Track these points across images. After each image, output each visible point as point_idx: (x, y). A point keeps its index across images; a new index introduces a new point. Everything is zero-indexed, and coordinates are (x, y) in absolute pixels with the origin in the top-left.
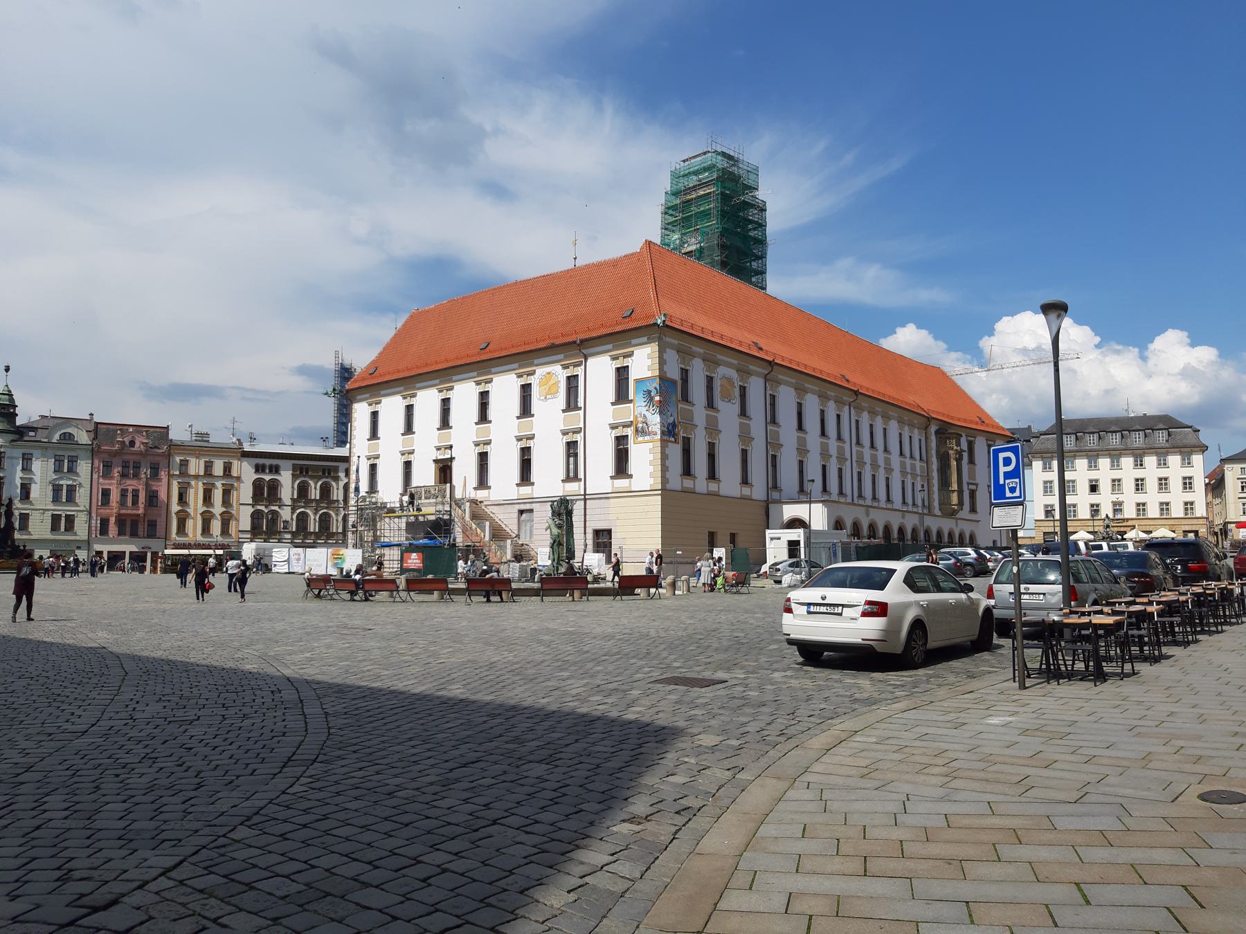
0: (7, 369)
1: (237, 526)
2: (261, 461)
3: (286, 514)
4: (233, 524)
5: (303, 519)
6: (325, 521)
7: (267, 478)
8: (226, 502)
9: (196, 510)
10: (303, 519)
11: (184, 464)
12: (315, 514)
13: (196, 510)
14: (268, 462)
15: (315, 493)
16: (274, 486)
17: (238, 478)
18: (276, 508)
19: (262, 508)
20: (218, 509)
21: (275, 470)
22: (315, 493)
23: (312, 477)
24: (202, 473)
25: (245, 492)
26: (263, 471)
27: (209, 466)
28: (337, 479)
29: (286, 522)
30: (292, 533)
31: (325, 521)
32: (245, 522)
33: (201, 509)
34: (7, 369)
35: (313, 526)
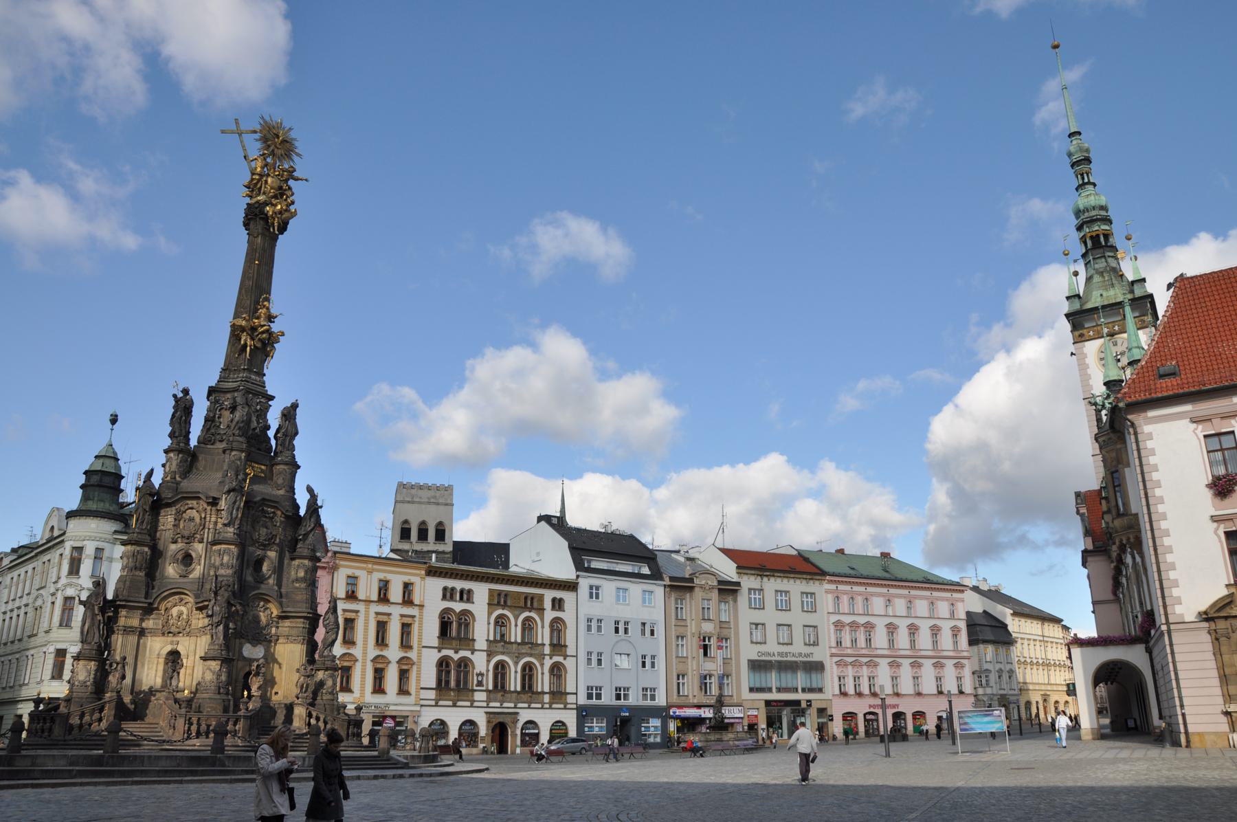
0: (114, 420)
1: (418, 680)
2: (450, 583)
3: (480, 663)
4: (413, 675)
5: (500, 669)
6: (528, 673)
7: (458, 607)
8: (405, 645)
9: (365, 653)
10: (500, 669)
11: (352, 581)
12: (516, 663)
13: (365, 653)
14: (459, 584)
15: (515, 633)
16: (465, 619)
17: (421, 606)
18: (466, 654)
19: (450, 653)
20: (393, 652)
21: (466, 596)
22: (515, 634)
23: (511, 608)
24: (375, 597)
25: (429, 630)
26: (452, 598)
27: (384, 587)
28: (541, 610)
29: (482, 675)
30: (487, 691)
31: (528, 673)
32: (428, 675)
33: (373, 652)
34: (114, 420)
35: (514, 682)
